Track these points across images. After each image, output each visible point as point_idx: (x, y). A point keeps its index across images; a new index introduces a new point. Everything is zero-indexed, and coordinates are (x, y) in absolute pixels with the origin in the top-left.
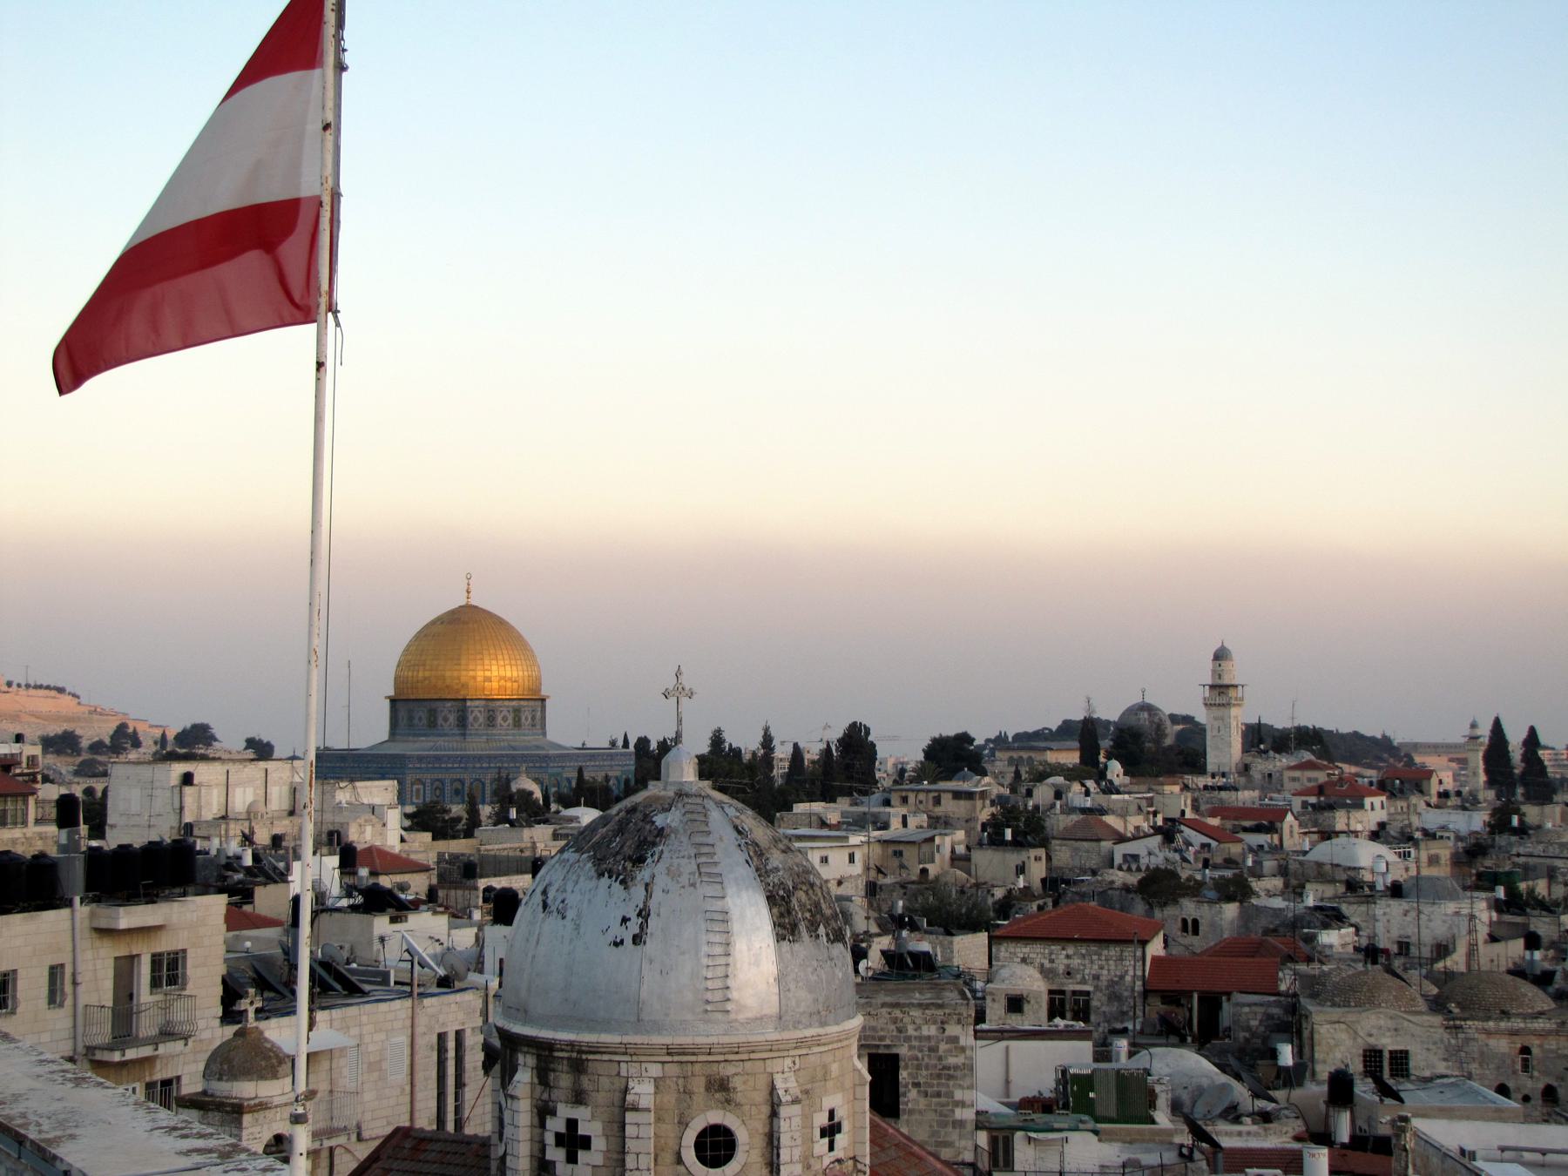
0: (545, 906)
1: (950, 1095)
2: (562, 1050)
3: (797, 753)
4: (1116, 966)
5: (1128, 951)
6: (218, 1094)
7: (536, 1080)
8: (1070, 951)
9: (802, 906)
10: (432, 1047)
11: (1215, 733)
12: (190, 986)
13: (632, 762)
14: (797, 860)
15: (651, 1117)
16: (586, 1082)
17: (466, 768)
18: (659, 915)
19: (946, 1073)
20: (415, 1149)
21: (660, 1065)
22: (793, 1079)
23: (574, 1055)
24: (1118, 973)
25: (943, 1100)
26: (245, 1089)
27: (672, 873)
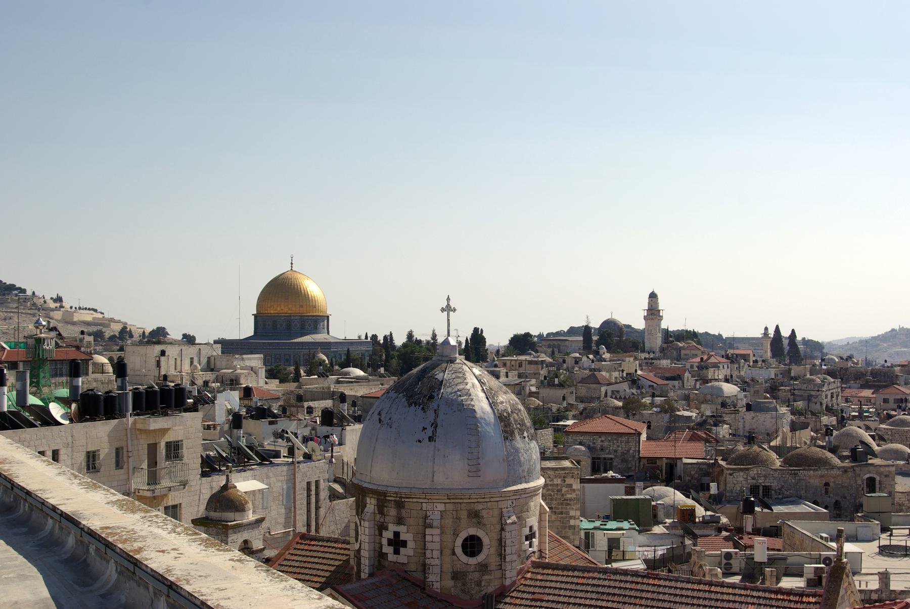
0: (380, 420)
1: (568, 513)
2: (391, 496)
7: (377, 512)
9: (516, 421)
10: (304, 488)
11: (649, 332)
17: (292, 349)
18: (442, 426)
21: (444, 504)
22: (512, 511)
24: (626, 449)
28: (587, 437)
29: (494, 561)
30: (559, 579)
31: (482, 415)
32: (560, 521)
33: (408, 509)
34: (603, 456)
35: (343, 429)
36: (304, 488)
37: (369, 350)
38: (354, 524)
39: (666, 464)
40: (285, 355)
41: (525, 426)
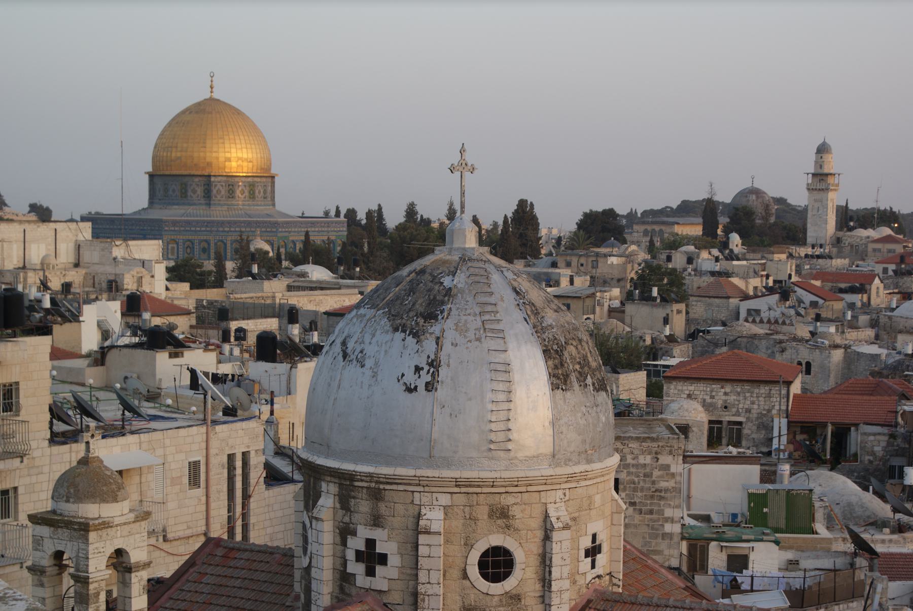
0: (345, 355)
1: (661, 512)
2: (362, 481)
5: (775, 390)
6: (66, 513)
7: (338, 506)
8: (728, 388)
9: (572, 358)
10: (223, 466)
11: (815, 212)
12: (22, 412)
13: (345, 229)
14: (568, 319)
15: (441, 539)
16: (383, 508)
17: (211, 231)
18: (448, 366)
20: (224, 556)
21: (449, 495)
22: (563, 508)
23: (373, 485)
24: (766, 407)
25: (654, 516)
26: (90, 510)
27: (461, 329)
29: (532, 589)
32: (648, 525)
33: (390, 502)
34: (727, 419)
40: (201, 241)
41: (590, 367)
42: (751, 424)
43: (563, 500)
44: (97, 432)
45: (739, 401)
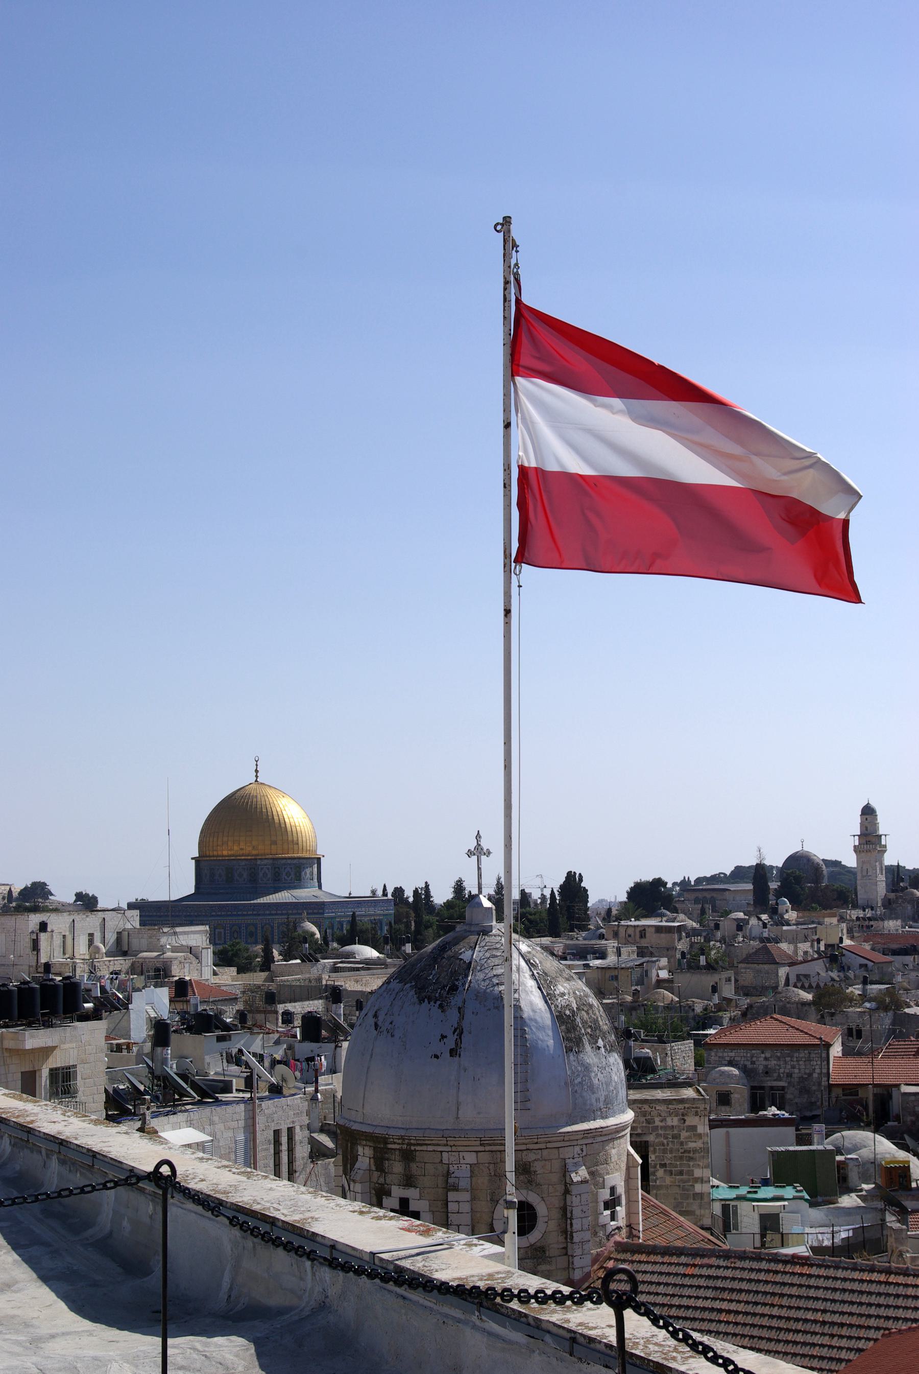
0: (376, 1025)
1: (691, 1173)
2: (395, 1143)
3: (524, 895)
4: (805, 1065)
7: (373, 1168)
8: (768, 1055)
9: (584, 1023)
11: (865, 873)
12: (80, 1094)
17: (259, 915)
19: (688, 1156)
24: (807, 1071)
25: (685, 1177)
28: (742, 1052)
29: (555, 1242)
30: (657, 1268)
31: (531, 1014)
32: (679, 1186)
33: (420, 1162)
34: (769, 1084)
35: (337, 1046)
36: (269, 1141)
37: (391, 914)
38: (341, 1188)
39: (875, 1095)
41: (600, 1031)
42: (794, 1089)
43: (581, 1155)
44: (152, 1104)
45: (779, 1066)
